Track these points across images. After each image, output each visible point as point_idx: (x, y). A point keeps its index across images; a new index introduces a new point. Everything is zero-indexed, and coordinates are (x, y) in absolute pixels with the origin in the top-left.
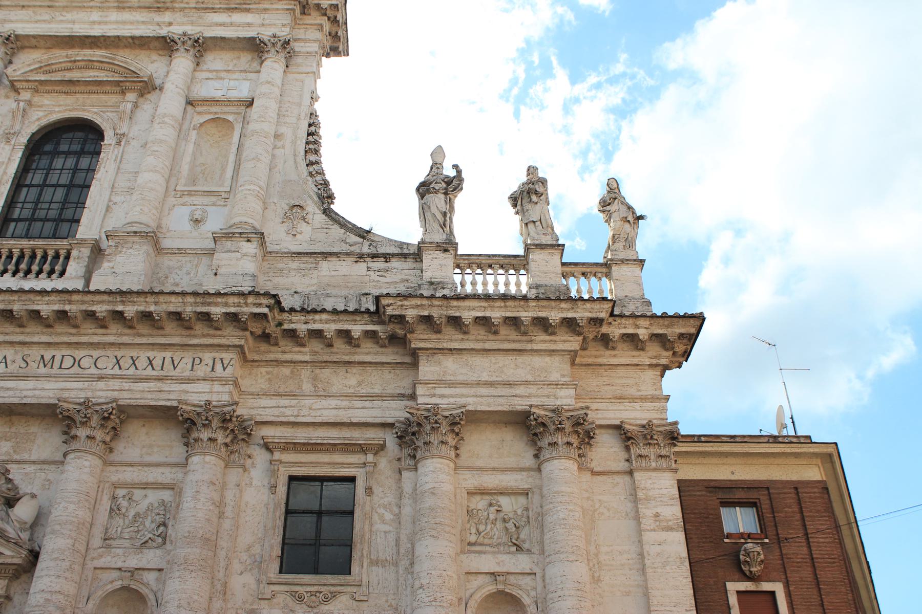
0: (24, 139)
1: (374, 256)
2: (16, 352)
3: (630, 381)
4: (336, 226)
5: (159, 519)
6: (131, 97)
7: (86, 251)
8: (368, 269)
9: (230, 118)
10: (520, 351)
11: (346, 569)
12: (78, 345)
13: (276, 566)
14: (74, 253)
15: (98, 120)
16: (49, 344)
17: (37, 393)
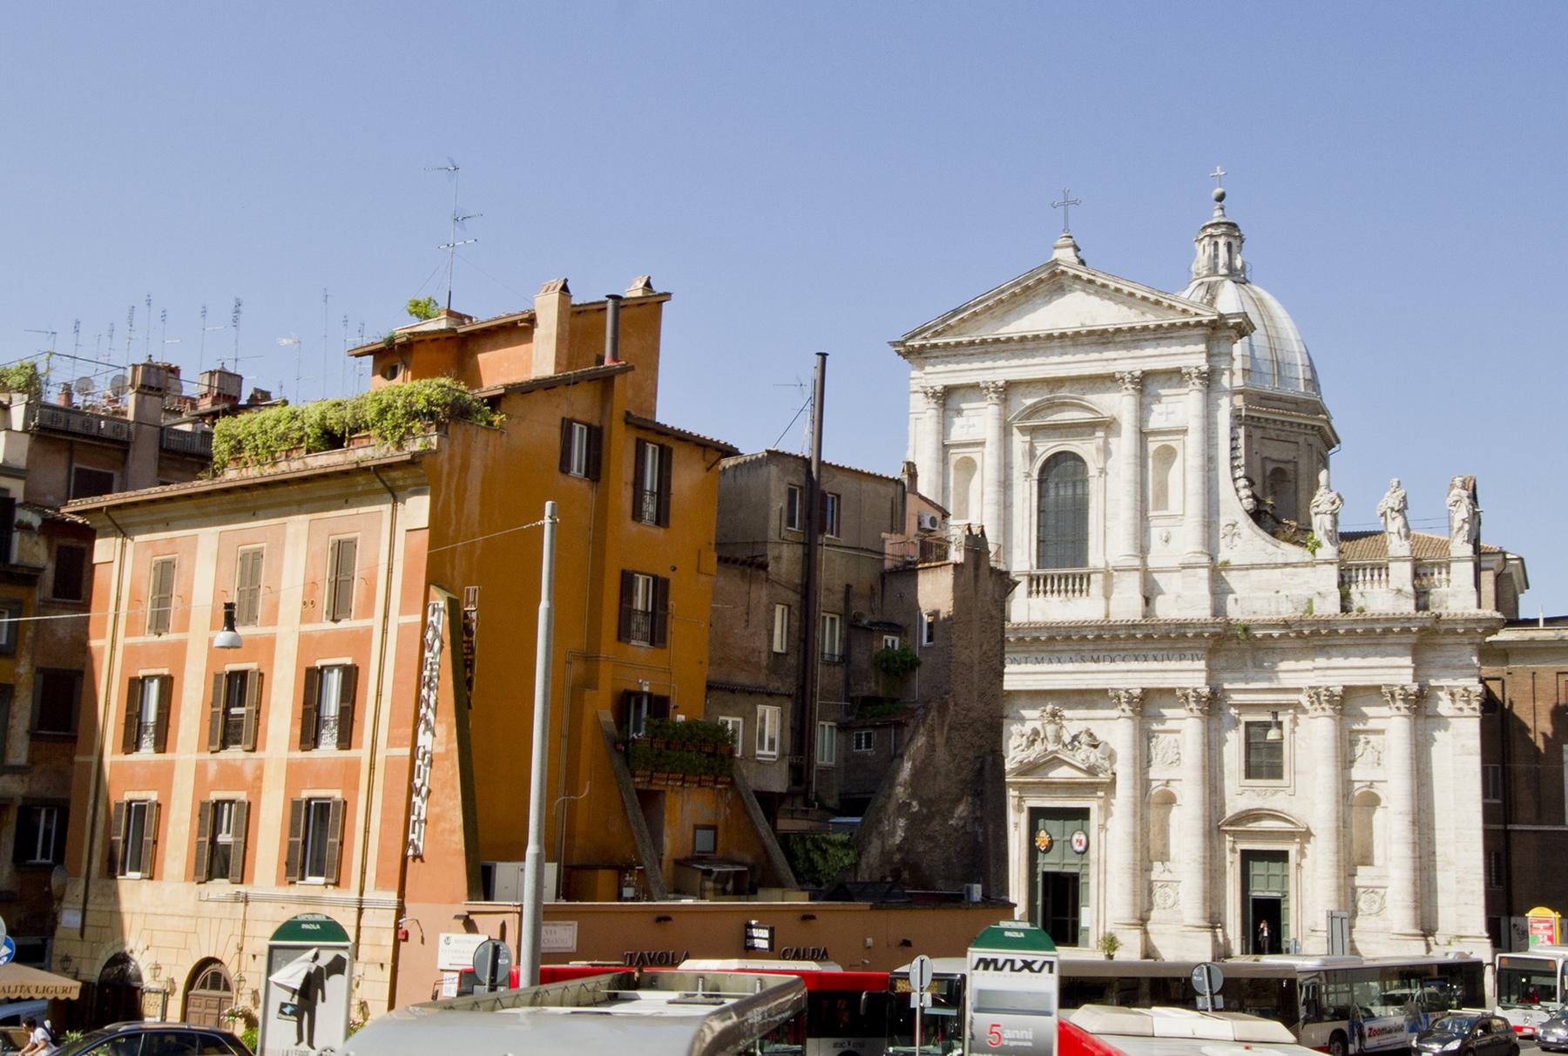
0: (1035, 475)
1: (1286, 565)
2: (1077, 655)
3: (1456, 654)
4: (1258, 538)
5: (1175, 750)
6: (1100, 434)
7: (1100, 576)
8: (1282, 574)
9: (1173, 444)
10: (1379, 644)
11: (1279, 776)
12: (1111, 650)
13: (1243, 774)
14: (1092, 577)
15: (1081, 453)
16: (1094, 650)
17: (1095, 681)
